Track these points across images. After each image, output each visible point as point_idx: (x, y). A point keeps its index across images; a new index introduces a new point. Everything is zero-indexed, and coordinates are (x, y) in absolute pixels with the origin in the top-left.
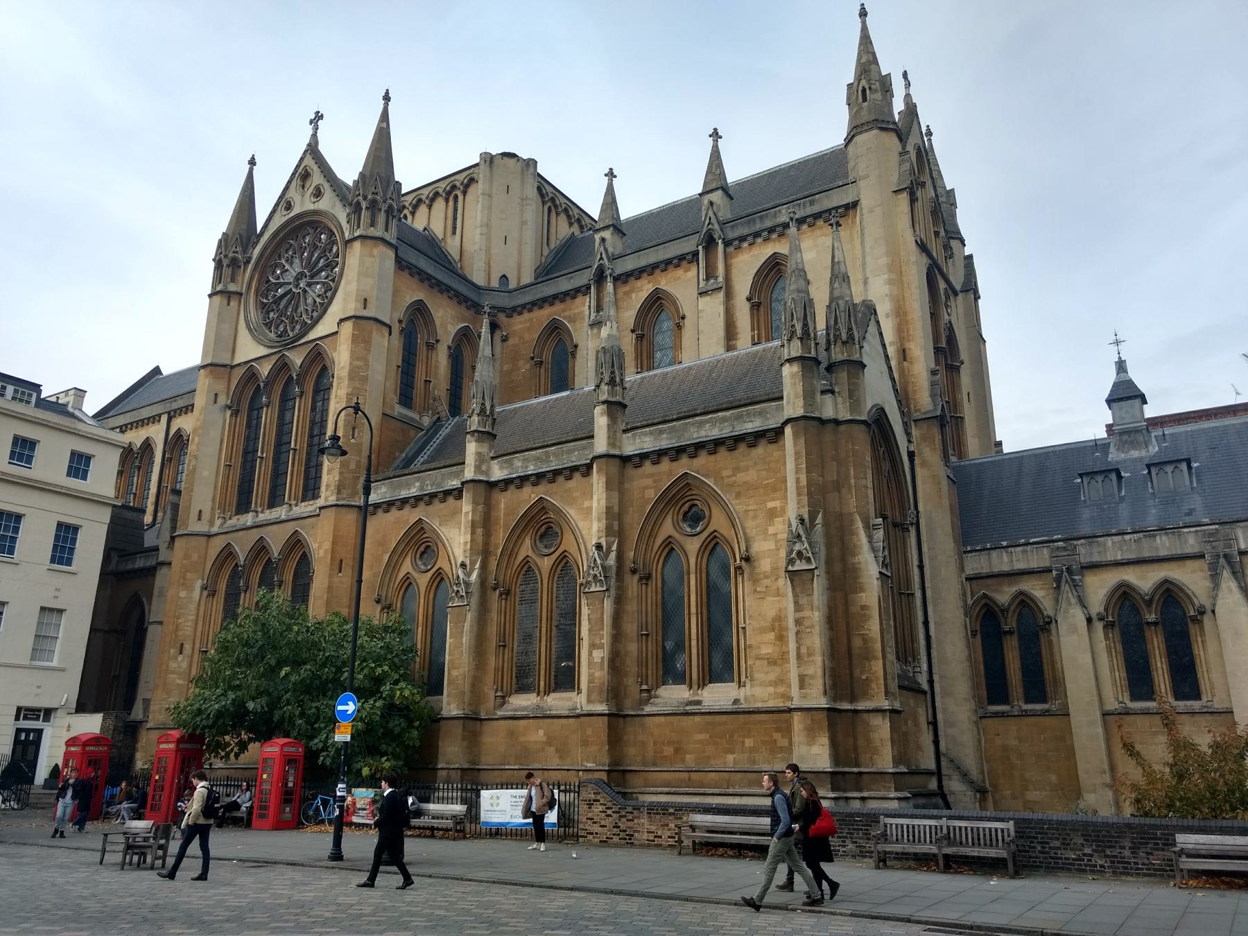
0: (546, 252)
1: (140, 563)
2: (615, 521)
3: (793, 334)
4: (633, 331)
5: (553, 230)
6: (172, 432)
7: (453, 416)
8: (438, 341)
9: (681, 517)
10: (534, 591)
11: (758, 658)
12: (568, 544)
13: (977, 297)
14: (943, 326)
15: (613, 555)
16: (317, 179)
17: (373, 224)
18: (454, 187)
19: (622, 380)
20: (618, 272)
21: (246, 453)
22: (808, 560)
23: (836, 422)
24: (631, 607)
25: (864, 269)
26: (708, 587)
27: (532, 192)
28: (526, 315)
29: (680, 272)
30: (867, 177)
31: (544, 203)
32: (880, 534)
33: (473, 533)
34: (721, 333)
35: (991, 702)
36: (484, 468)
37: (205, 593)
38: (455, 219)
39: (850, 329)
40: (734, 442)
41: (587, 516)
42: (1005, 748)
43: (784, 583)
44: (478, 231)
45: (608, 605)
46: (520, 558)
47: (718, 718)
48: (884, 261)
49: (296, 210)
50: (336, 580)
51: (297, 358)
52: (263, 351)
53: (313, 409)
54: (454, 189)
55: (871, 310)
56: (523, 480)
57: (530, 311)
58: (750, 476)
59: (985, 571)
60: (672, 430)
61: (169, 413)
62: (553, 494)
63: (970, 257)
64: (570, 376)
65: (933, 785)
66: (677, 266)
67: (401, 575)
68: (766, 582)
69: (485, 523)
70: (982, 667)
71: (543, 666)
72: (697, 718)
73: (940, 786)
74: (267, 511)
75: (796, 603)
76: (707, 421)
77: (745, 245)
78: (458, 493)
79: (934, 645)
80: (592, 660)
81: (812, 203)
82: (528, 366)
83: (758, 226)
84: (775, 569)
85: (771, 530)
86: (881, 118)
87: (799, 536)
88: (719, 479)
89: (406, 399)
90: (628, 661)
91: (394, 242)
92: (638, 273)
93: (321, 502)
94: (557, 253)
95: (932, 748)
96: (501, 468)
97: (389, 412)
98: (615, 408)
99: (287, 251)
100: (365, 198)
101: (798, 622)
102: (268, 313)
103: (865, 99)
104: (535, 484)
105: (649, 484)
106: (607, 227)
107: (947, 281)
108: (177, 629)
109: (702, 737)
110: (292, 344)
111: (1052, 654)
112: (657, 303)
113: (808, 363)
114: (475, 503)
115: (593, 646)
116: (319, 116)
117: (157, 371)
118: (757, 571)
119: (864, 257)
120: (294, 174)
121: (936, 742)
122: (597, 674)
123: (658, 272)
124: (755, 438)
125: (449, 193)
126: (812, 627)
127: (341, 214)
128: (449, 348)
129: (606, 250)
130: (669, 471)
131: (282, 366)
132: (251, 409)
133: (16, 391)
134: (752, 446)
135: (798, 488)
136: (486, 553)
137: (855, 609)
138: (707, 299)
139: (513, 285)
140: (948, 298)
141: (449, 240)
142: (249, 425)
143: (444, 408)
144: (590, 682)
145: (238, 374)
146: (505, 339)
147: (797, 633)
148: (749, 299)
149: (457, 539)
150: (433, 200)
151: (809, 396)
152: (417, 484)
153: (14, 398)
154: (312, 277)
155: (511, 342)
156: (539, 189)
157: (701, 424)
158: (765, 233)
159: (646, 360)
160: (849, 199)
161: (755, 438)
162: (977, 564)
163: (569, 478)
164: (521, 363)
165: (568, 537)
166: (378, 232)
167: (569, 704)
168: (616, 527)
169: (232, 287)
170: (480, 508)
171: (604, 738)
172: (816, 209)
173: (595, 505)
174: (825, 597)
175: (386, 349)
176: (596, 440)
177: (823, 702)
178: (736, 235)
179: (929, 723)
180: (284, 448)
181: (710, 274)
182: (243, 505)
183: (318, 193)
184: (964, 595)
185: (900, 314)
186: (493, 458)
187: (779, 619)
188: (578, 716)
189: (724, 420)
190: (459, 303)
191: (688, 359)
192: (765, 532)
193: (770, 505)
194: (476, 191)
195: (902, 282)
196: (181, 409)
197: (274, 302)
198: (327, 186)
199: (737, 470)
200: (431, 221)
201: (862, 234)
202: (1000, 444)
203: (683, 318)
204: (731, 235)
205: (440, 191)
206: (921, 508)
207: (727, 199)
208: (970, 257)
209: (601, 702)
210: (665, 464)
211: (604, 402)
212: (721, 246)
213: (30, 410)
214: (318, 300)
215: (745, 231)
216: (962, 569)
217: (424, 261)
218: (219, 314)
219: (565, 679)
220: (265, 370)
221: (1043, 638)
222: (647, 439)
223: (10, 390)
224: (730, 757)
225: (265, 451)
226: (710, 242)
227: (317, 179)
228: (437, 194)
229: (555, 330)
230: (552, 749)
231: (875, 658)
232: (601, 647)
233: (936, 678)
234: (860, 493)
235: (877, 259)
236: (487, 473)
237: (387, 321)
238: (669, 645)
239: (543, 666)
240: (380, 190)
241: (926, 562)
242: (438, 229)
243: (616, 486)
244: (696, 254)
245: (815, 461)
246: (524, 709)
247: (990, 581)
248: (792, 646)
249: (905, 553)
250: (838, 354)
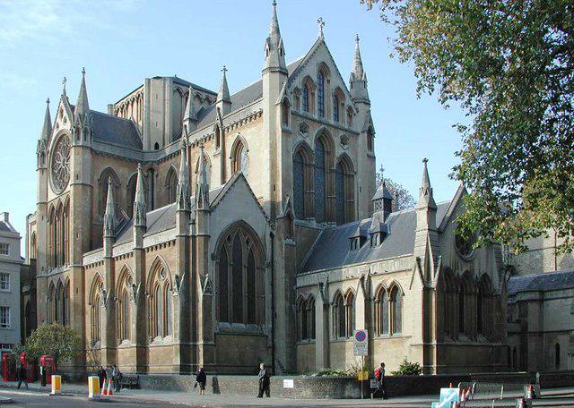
220: (56, 204)
237: (89, 183)
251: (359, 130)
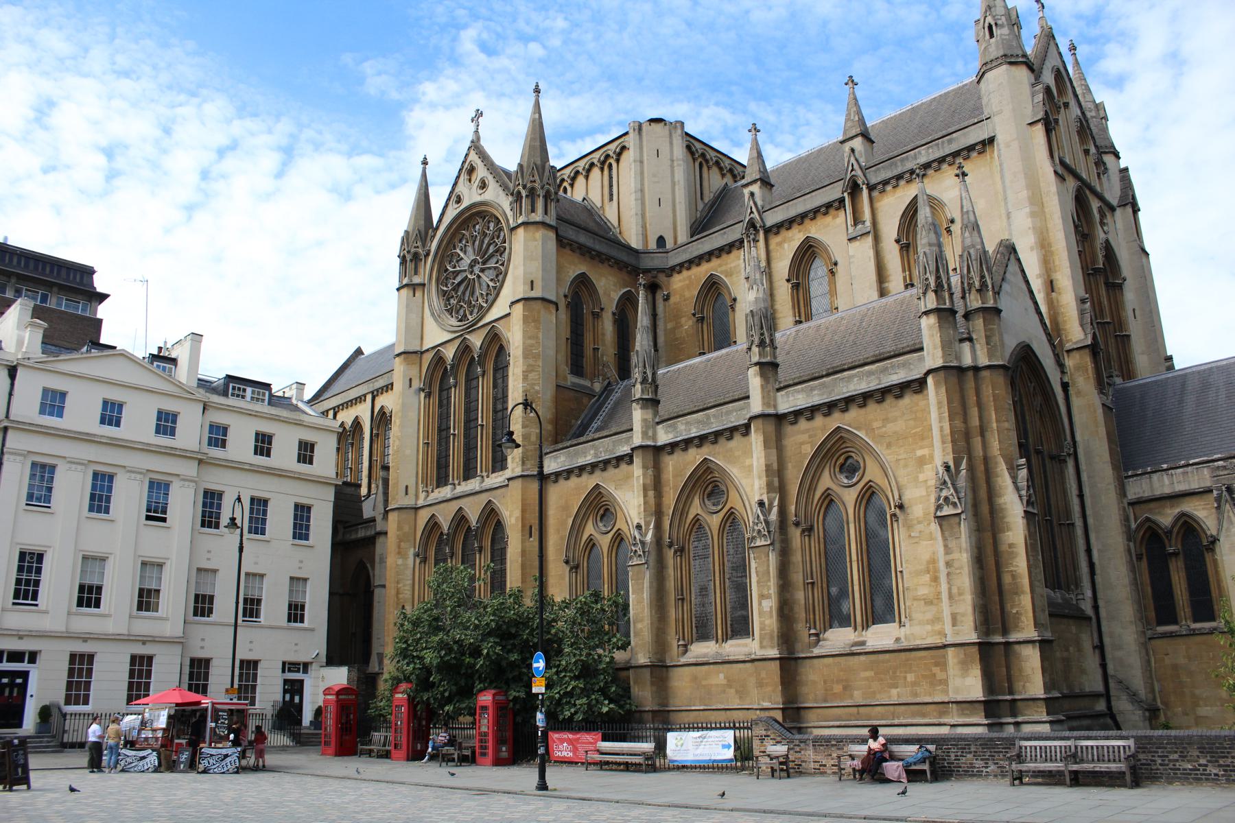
0: (701, 206)
1: (361, 534)
2: (777, 477)
3: (927, 286)
4: (788, 281)
5: (705, 184)
6: (377, 410)
7: (622, 379)
8: (602, 309)
9: (837, 470)
10: (706, 547)
11: (915, 599)
12: (734, 501)
13: (1136, 210)
14: (1099, 246)
15: (775, 510)
16: (481, 172)
17: (533, 211)
18: (608, 156)
19: (772, 341)
20: (769, 224)
21: (440, 430)
22: (955, 505)
23: (976, 369)
24: (797, 558)
25: (1006, 203)
26: (867, 535)
27: (679, 150)
28: (685, 273)
29: (828, 219)
30: (1000, 112)
31: (694, 160)
32: (1023, 473)
33: (645, 496)
35: (1160, 623)
36: (650, 433)
37: (418, 561)
38: (611, 186)
39: (982, 277)
40: (883, 394)
41: (748, 472)
42: (1175, 667)
43: (935, 527)
44: (633, 197)
45: (773, 558)
46: (691, 516)
47: (881, 657)
48: (1024, 194)
49: (465, 204)
50: (527, 544)
51: (476, 340)
52: (449, 336)
53: (495, 386)
54: (607, 159)
55: (1010, 250)
56: (687, 443)
57: (689, 269)
58: (899, 426)
59: (1147, 494)
60: (824, 385)
61: (372, 392)
62: (716, 454)
63: (1126, 169)
64: (732, 328)
65: (1101, 706)
66: (826, 214)
67: (585, 537)
69: (656, 485)
70: (1149, 589)
71: (719, 616)
72: (862, 658)
73: (1109, 707)
74: (463, 483)
75: (946, 546)
77: (889, 188)
78: (628, 458)
79: (1098, 571)
80: (763, 608)
81: (950, 142)
82: (690, 323)
83: (899, 170)
84: (926, 514)
85: (922, 477)
86: (1009, 53)
87: (945, 483)
88: (870, 431)
89: (577, 367)
90: (796, 609)
91: (553, 223)
92: (789, 224)
93: (508, 473)
94: (712, 206)
95: (1099, 671)
96: (666, 432)
97: (562, 383)
98: (769, 368)
99: (460, 241)
100: (524, 187)
101: (948, 564)
102: (448, 300)
103: (992, 35)
104: (699, 446)
105: (804, 440)
106: (754, 182)
107: (1097, 199)
108: (398, 593)
110: (471, 328)
111: (1217, 572)
112: (808, 252)
113: (945, 314)
114: (645, 467)
115: (762, 597)
116: (479, 114)
117: (359, 352)
118: (911, 517)
119: (1005, 191)
120: (461, 170)
121: (1104, 666)
122: (767, 622)
123: (807, 221)
124: (901, 389)
125: (603, 163)
126: (961, 568)
127: (505, 202)
128: (614, 314)
129: (755, 204)
130: (822, 427)
131: (465, 349)
132: (441, 390)
133: (253, 392)
134: (899, 397)
135: (942, 436)
136: (659, 513)
137: (1004, 548)
138: (856, 244)
139: (669, 244)
140: (1103, 215)
141: (607, 208)
142: (440, 406)
143: (613, 373)
144: (761, 629)
145: (428, 358)
146: (667, 298)
147: (948, 574)
148: (897, 241)
149: (631, 502)
150: (589, 171)
151: (946, 346)
153: (252, 398)
154: (484, 263)
155: (672, 300)
156: (688, 147)
157: (850, 378)
158: (908, 175)
159: (803, 312)
160: (986, 136)
161: (901, 389)
162: (1138, 488)
163: (730, 438)
164: (683, 320)
165: (733, 494)
166: (538, 216)
167: (746, 650)
168: (776, 484)
169: (417, 280)
170: (650, 472)
171: (777, 679)
172: (954, 147)
173: (755, 464)
174: (974, 539)
175: (555, 323)
176: (751, 400)
177: (973, 637)
178: (879, 179)
179: (1094, 648)
180: (472, 425)
181: (857, 221)
182: (442, 480)
183: (483, 185)
184: (1127, 519)
185: (1044, 245)
186: (658, 423)
187: (933, 561)
188: (753, 661)
189: (870, 373)
190: (620, 269)
191: (842, 302)
193: (919, 453)
194: (628, 157)
195: (1044, 212)
196: (382, 388)
197: (453, 289)
198: (490, 177)
199: (886, 420)
200: (588, 191)
201: (1002, 170)
202: (1170, 358)
203: (836, 264)
204: (874, 180)
205: (595, 161)
206: (1078, 438)
207: (868, 144)
208: (1126, 169)
209: (773, 647)
210: (819, 420)
211: (756, 364)
212: (865, 192)
213: (263, 408)
214: (491, 284)
215: (889, 174)
216: (1122, 492)
217: (582, 236)
218: (407, 306)
219: (740, 627)
220: (449, 353)
221: (1208, 557)
222: (800, 396)
223: (249, 390)
224: (894, 692)
225: (456, 428)
226: (854, 189)
227: (481, 172)
228: (592, 165)
229: (713, 287)
230: (733, 691)
231: (1023, 592)
233: (1101, 603)
234: (999, 438)
235: (1018, 193)
236: (654, 438)
237: (553, 298)
238: (834, 590)
239: (719, 616)
240: (537, 177)
241: (1086, 491)
242: (596, 197)
243: (776, 443)
244: (842, 200)
245: (959, 409)
246: (705, 655)
247: (1152, 505)
248: (944, 587)
249: (1063, 483)
250: (975, 302)
251: (1115, 202)
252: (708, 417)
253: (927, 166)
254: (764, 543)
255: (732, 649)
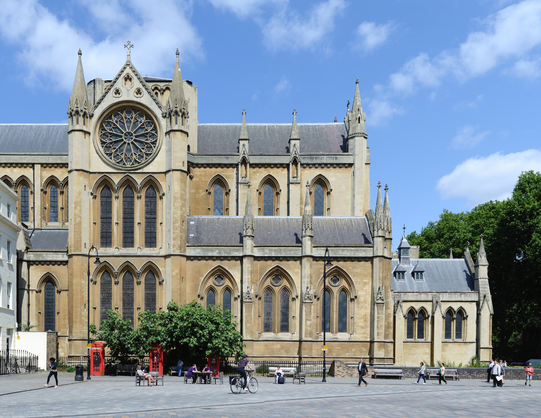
34: (299, 202)
57: (205, 168)
68: (362, 304)
72: (337, 343)
76: (346, 250)
83: (315, 161)
85: (364, 288)
96: (259, 251)
109: (338, 348)
135: (379, 278)
152: (217, 251)
157: (343, 250)
164: (200, 191)
187: (365, 315)
192: (362, 289)
193: (365, 281)
199: (354, 267)
224: (347, 354)
230: (283, 351)
232: (310, 320)
252: (280, 250)
253: (326, 165)
254: (309, 301)
255: (282, 336)
